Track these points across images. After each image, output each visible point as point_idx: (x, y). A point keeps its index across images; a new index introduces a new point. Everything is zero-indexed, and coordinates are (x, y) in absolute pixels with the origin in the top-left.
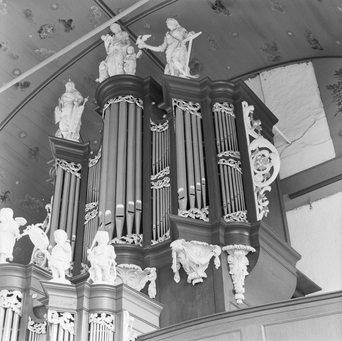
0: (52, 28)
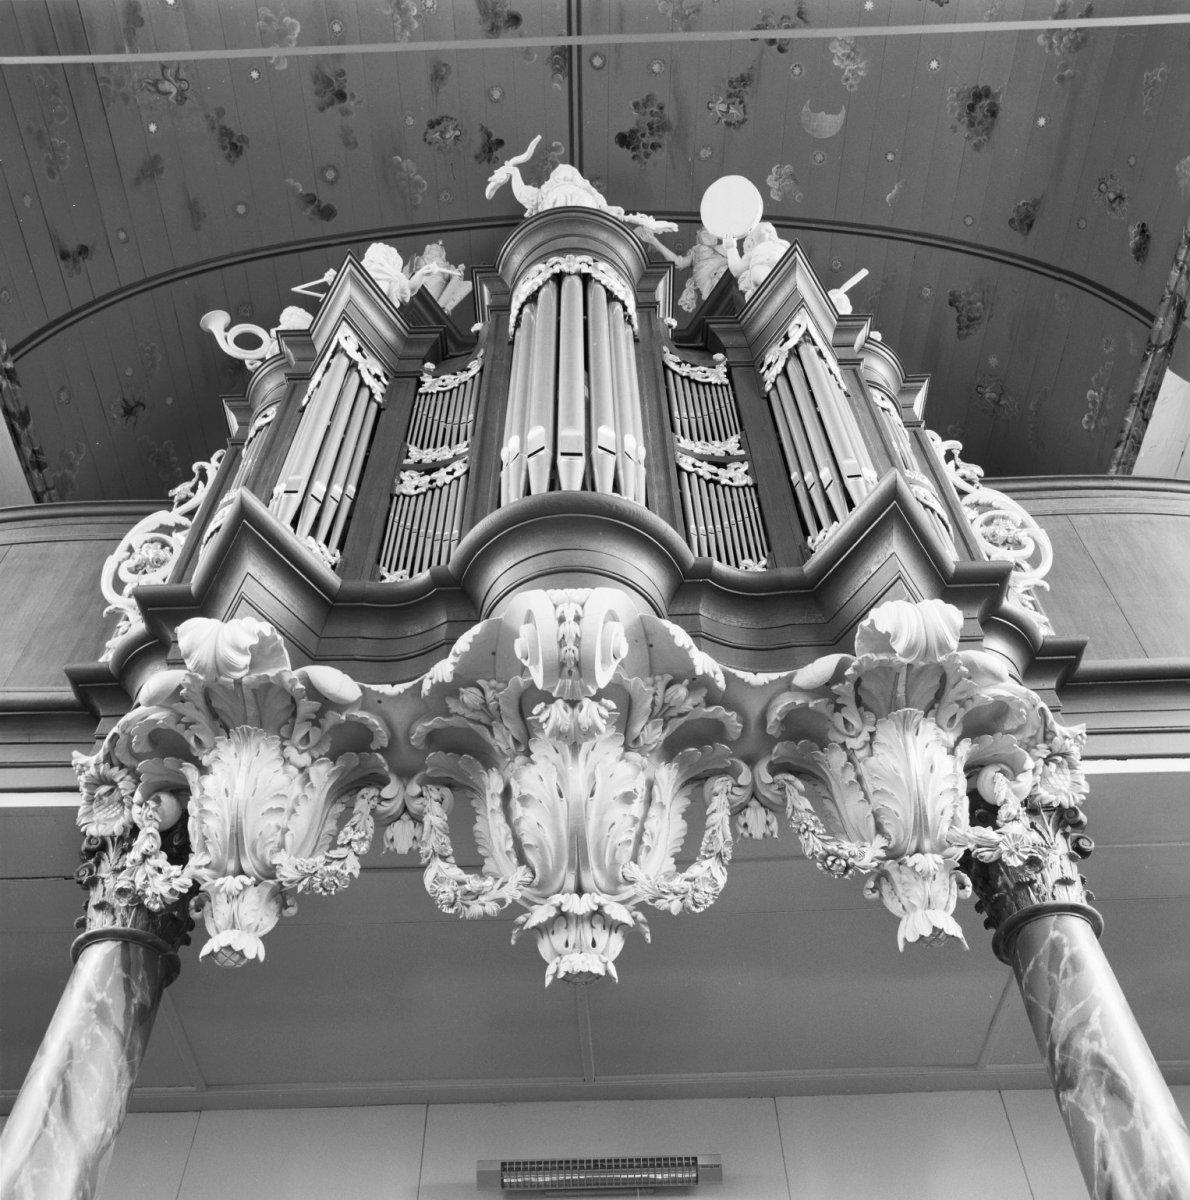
0: (458, 133)
